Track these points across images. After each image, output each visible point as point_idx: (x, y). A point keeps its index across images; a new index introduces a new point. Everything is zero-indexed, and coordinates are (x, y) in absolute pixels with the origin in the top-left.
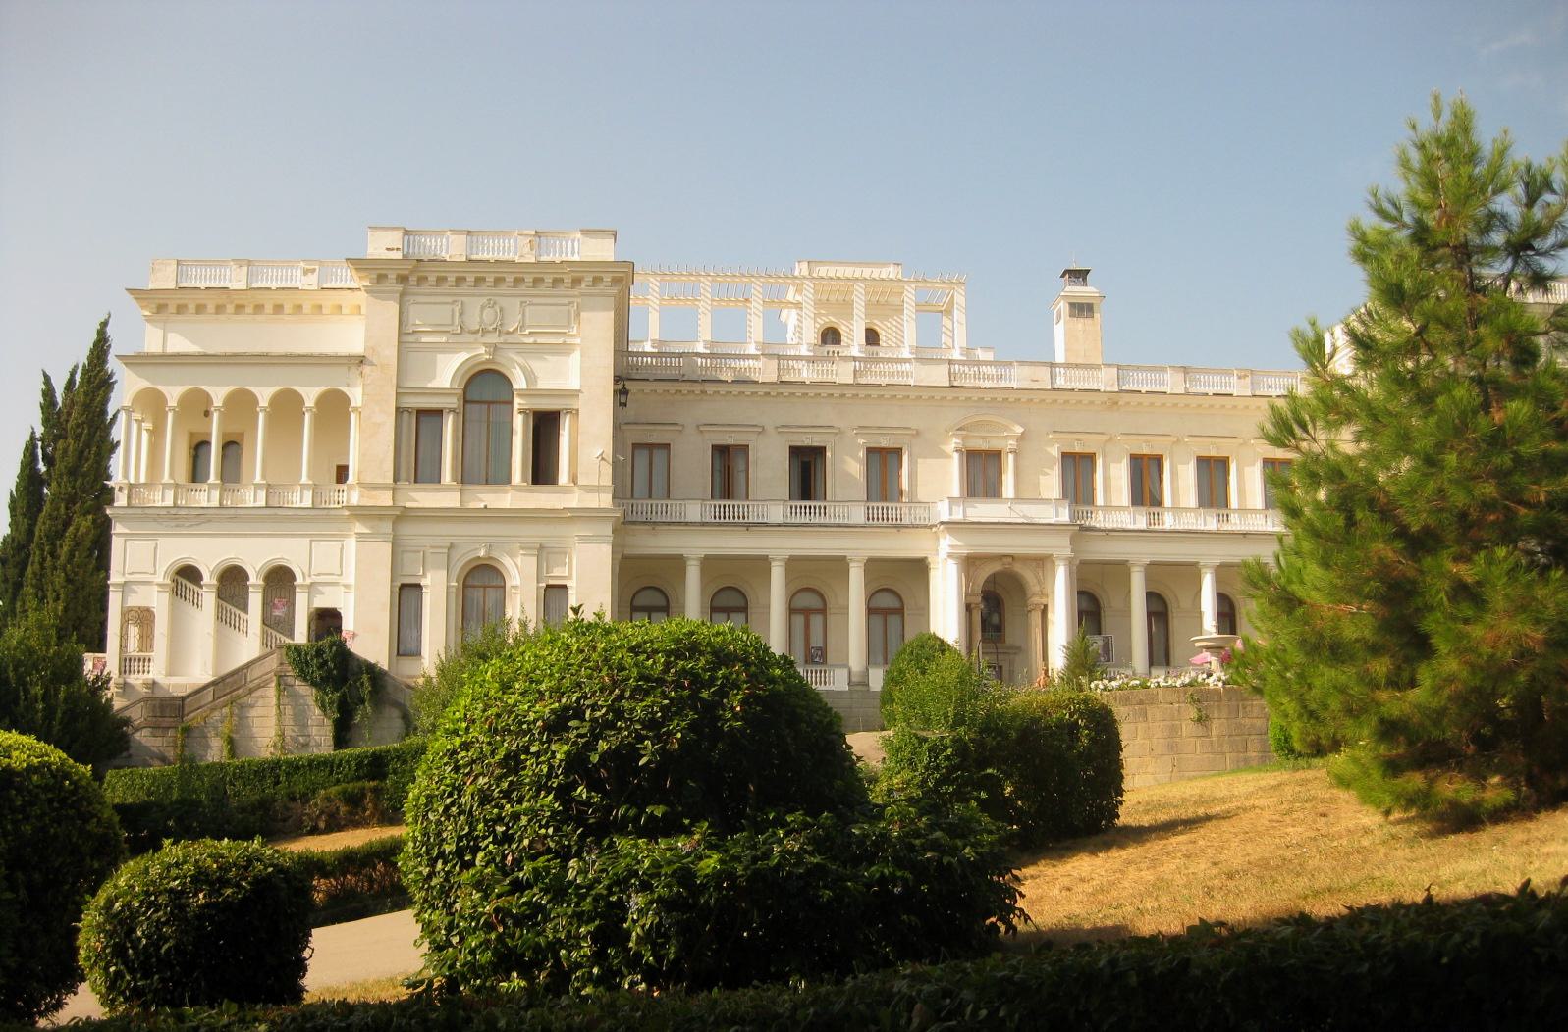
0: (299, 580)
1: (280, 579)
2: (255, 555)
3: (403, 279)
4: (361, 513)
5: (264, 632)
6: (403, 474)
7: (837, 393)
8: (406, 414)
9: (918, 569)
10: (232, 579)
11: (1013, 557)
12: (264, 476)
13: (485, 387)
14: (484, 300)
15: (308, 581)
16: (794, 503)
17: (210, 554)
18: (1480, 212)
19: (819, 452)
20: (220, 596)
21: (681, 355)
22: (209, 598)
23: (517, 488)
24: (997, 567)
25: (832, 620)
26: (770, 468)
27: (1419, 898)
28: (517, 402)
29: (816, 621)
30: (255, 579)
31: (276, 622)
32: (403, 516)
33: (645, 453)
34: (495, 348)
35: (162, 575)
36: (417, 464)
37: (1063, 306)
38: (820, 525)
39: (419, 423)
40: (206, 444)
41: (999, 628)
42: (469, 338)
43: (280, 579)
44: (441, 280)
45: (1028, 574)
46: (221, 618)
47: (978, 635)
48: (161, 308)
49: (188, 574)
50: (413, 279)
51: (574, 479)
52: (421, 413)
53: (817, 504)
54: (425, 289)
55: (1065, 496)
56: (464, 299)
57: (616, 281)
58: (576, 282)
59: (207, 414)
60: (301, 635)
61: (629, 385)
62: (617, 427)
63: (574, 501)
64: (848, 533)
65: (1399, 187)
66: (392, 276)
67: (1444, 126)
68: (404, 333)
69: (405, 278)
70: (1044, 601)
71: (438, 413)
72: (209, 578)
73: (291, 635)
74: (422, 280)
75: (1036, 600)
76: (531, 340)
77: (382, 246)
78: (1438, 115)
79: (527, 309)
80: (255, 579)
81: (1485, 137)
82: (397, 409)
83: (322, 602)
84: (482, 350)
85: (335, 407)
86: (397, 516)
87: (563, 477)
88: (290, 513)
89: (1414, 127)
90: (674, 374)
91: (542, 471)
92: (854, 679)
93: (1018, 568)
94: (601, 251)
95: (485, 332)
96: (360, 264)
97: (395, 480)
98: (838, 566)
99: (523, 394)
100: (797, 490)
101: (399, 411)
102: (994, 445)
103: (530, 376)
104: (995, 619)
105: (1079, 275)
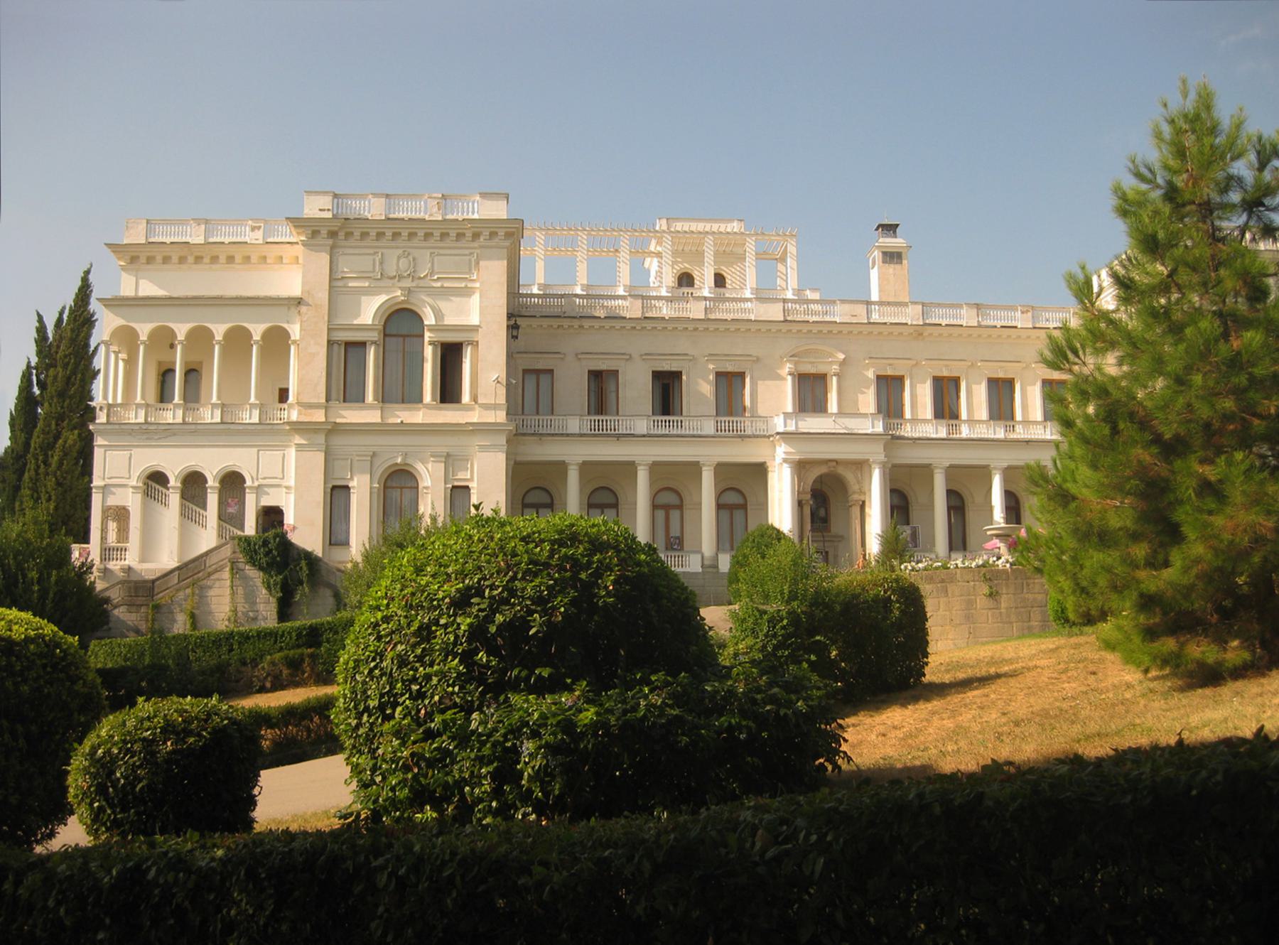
0: (248, 483)
1: (233, 482)
2: (213, 462)
3: (333, 234)
5: (219, 526)
6: (334, 395)
7: (691, 327)
8: (336, 346)
9: (759, 472)
10: (193, 483)
11: (836, 461)
12: (219, 398)
13: (401, 323)
14: (400, 251)
15: (256, 484)
16: (656, 418)
18: (1220, 175)
19: (678, 375)
20: (183, 497)
21: (562, 296)
22: (174, 499)
23: (428, 406)
24: (823, 470)
25: (687, 514)
26: (636, 388)
27: (1173, 741)
29: (675, 515)
30: (212, 482)
31: (230, 517)
32: (333, 430)
33: (534, 377)
34: (409, 291)
36: (345, 385)
37: (877, 254)
38: (678, 436)
39: (346, 353)
40: (172, 371)
41: (825, 520)
42: (390, 283)
43: (233, 482)
44: (364, 235)
45: (849, 476)
46: (185, 514)
47: (808, 526)
48: (133, 260)
49: (157, 478)
50: (341, 235)
52: (349, 345)
53: (675, 418)
54: (351, 242)
55: (879, 411)
57: (509, 235)
58: (476, 236)
59: (172, 346)
60: (250, 528)
61: (520, 321)
62: (510, 356)
63: (475, 417)
64: (700, 441)
65: (1153, 155)
66: (324, 232)
67: (1190, 104)
68: (335, 279)
69: (334, 234)
70: (862, 498)
71: (363, 345)
73: (242, 528)
74: (349, 235)
75: (856, 497)
76: (439, 284)
77: (316, 207)
78: (1185, 95)
79: (436, 259)
80: (212, 482)
81: (1224, 113)
82: (329, 341)
83: (267, 501)
84: (399, 293)
85: (277, 341)
87: (466, 398)
88: (241, 427)
89: (1165, 105)
90: (557, 311)
91: (449, 392)
92: (706, 563)
94: (497, 210)
95: (401, 277)
96: (298, 223)
97: (327, 401)
98: (693, 469)
99: (431, 329)
100: (659, 407)
101: (330, 343)
102: (821, 369)
103: (438, 314)
104: (822, 513)
105: (890, 229)
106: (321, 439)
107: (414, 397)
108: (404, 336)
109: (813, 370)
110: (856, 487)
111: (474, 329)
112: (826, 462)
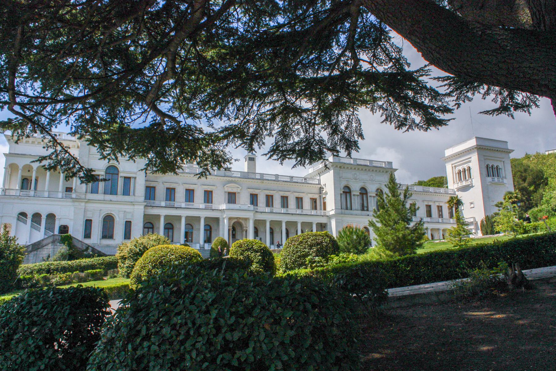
1: (51, 217)
2: (44, 210)
5: (45, 231)
10: (37, 217)
11: (240, 218)
17: (30, 209)
20: (32, 221)
22: (29, 220)
24: (236, 220)
45: (243, 222)
51: (134, 195)
60: (56, 232)
87: (131, 193)
91: (126, 192)
93: (241, 221)
97: (86, 192)
100: (206, 201)
108: (112, 174)
109: (232, 191)
110: (245, 226)
112: (237, 218)
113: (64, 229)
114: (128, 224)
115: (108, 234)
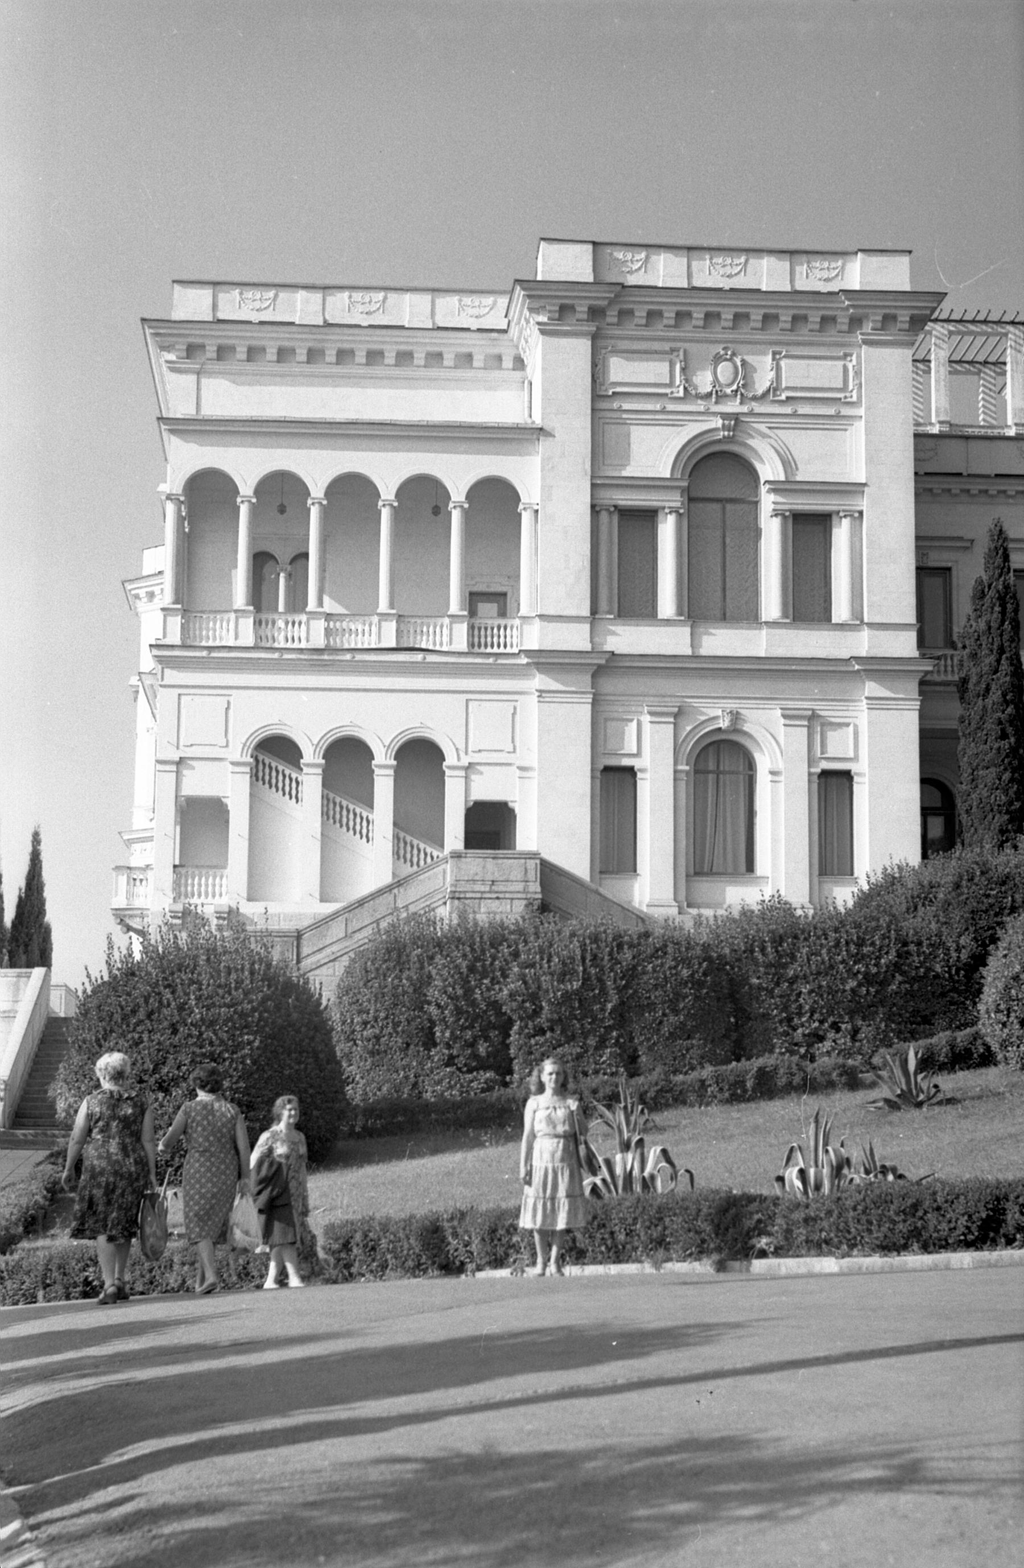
0: (450, 759)
1: (420, 757)
2: (382, 718)
3: (595, 313)
4: (545, 661)
5: (396, 838)
6: (603, 605)
10: (347, 756)
12: (392, 605)
15: (465, 761)
17: (311, 716)
22: (311, 783)
23: (772, 624)
28: (767, 501)
30: (383, 757)
31: (417, 822)
34: (736, 421)
35: (239, 750)
36: (620, 584)
39: (621, 527)
40: (305, 556)
42: (700, 406)
44: (653, 315)
46: (329, 813)
48: (192, 350)
54: (629, 329)
56: (687, 345)
63: (863, 644)
68: (600, 393)
69: (600, 313)
72: (311, 755)
74: (625, 314)
76: (788, 410)
77: (567, 264)
79: (783, 363)
80: (383, 757)
82: (593, 507)
83: (487, 788)
84: (719, 423)
86: (600, 667)
91: (808, 599)
94: (894, 275)
96: (538, 292)
97: (594, 611)
99: (777, 488)
103: (788, 464)
106: (585, 680)
107: (747, 614)
111: (856, 489)
113: (490, 826)
114: (833, 787)
115: (717, 840)
